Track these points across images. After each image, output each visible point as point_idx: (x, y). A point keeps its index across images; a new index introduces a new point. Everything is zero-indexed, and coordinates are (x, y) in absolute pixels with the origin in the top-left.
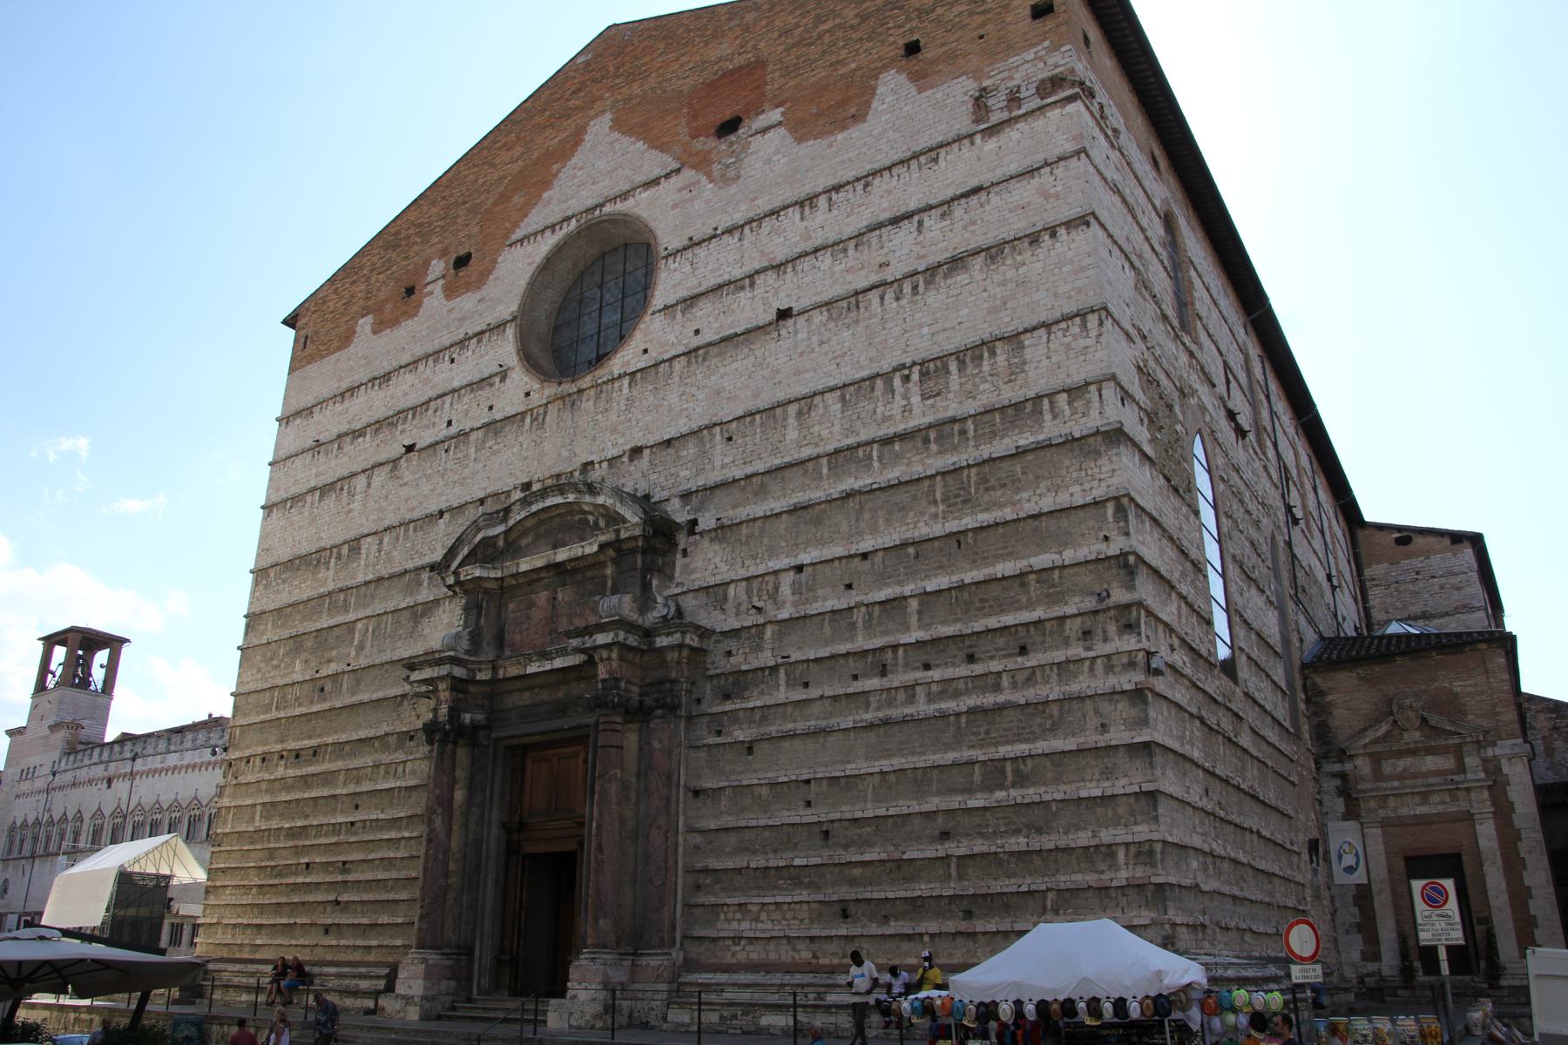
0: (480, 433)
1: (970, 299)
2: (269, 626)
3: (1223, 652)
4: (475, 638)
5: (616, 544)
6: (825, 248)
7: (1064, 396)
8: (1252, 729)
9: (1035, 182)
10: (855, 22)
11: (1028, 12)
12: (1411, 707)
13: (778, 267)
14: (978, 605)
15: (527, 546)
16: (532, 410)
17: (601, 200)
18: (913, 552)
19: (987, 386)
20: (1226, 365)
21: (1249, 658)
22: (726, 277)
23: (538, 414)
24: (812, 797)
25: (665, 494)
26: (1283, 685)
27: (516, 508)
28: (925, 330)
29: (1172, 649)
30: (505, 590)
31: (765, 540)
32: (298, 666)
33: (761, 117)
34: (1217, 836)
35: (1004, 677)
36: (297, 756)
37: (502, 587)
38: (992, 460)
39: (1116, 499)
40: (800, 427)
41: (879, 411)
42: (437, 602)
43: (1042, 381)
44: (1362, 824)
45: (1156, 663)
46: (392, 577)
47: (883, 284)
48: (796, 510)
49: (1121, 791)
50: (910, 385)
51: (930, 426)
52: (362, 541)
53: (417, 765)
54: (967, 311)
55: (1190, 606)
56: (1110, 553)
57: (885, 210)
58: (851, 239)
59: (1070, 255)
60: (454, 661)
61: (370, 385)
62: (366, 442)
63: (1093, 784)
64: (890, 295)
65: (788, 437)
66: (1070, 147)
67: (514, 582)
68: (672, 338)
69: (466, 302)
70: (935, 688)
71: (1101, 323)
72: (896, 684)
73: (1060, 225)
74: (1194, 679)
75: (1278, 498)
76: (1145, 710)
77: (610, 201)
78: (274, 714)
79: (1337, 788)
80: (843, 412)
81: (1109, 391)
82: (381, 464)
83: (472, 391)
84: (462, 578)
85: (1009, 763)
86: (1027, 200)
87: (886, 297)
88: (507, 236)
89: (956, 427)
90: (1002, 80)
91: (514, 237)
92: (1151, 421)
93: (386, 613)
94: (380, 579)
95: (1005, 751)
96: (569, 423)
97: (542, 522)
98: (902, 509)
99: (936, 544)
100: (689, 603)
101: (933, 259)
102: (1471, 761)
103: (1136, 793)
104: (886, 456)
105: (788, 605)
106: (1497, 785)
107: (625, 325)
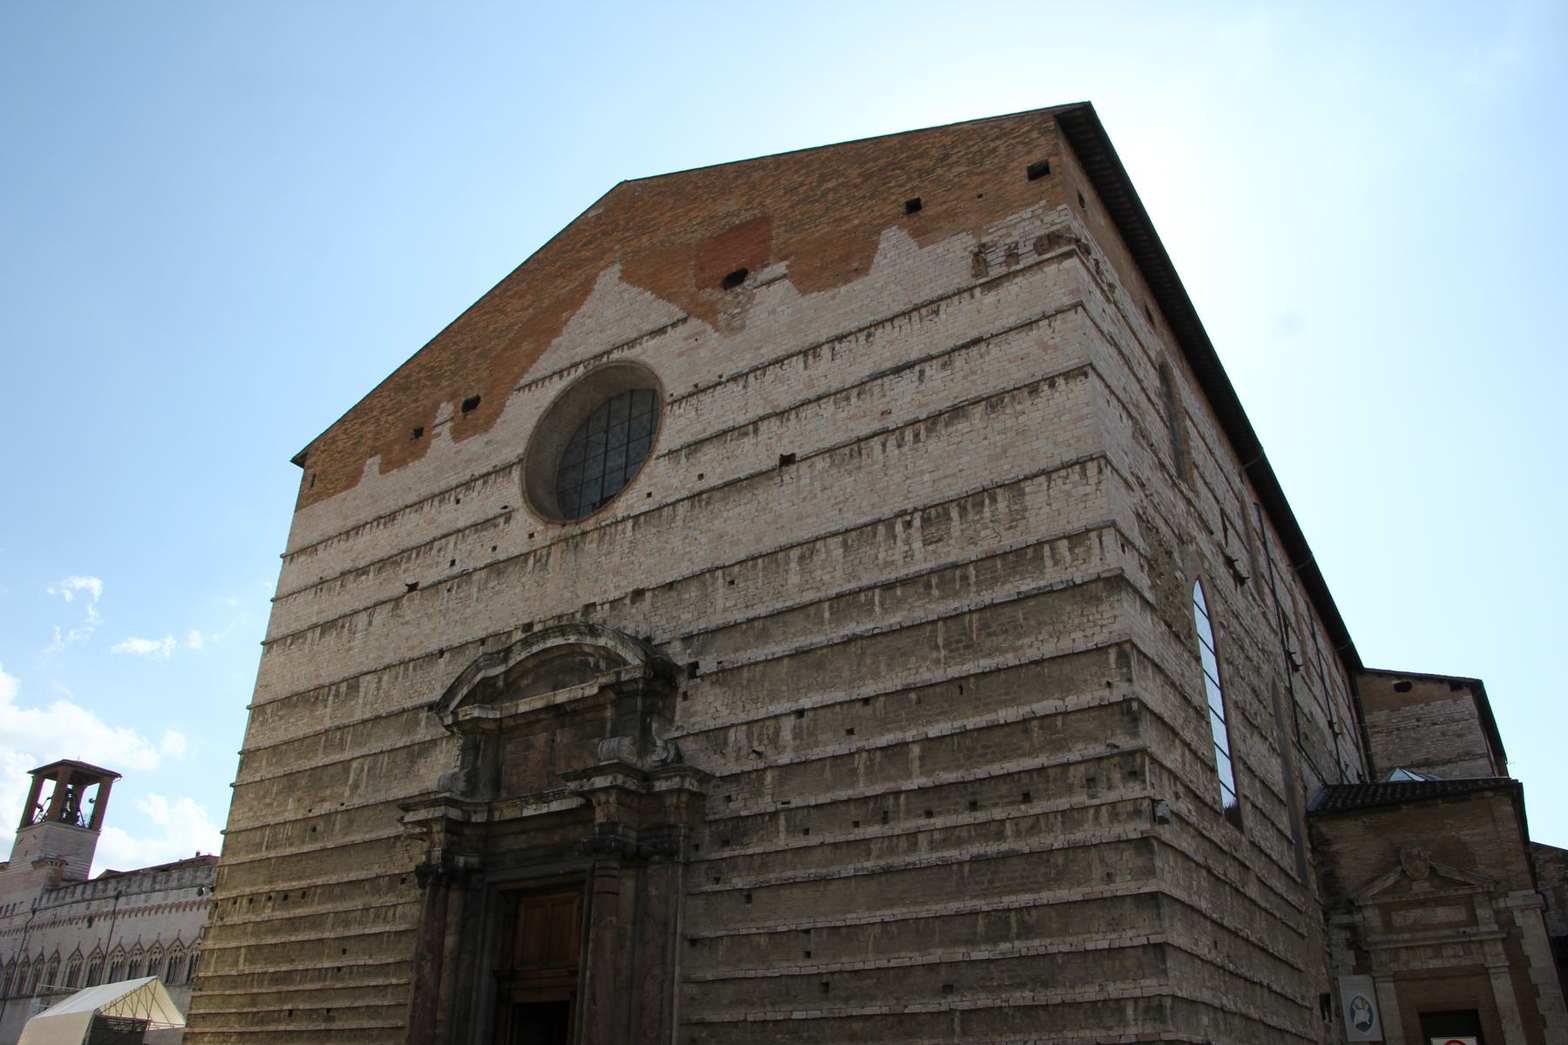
0: (483, 574)
1: (971, 447)
2: (264, 763)
3: (1228, 799)
4: (472, 779)
5: (617, 687)
6: (828, 395)
7: (1065, 543)
8: (1258, 879)
9: (1034, 333)
10: (858, 181)
11: (1025, 173)
12: (1419, 856)
13: (782, 415)
14: (980, 751)
15: (528, 686)
16: (535, 551)
17: (609, 347)
18: (915, 698)
19: (988, 532)
20: (1222, 510)
21: (1254, 806)
22: (730, 424)
23: (541, 556)
24: (811, 947)
25: (667, 637)
26: (1289, 834)
27: (517, 648)
28: (927, 477)
29: (1177, 797)
30: (503, 730)
31: (767, 684)
32: (291, 805)
33: (766, 270)
34: (1226, 991)
35: (1008, 825)
36: (286, 898)
37: (500, 729)
38: (993, 606)
39: (1119, 645)
40: (802, 572)
41: (881, 556)
42: (433, 742)
43: (1043, 528)
44: (1374, 978)
45: (1161, 811)
46: (390, 716)
47: (886, 432)
48: (798, 654)
49: (1128, 944)
50: (911, 531)
51: (932, 572)
52: (362, 679)
53: (407, 909)
54: (968, 458)
55: (1194, 753)
56: (1113, 699)
57: (887, 360)
58: (853, 387)
59: (1068, 404)
60: (449, 802)
61: (375, 524)
62: (369, 580)
63: (1100, 936)
64: (892, 442)
65: (790, 582)
66: (1068, 301)
67: (513, 723)
68: (675, 482)
69: (474, 444)
70: (937, 836)
71: (1100, 471)
72: (897, 831)
73: (1058, 376)
74: (1200, 827)
75: (1278, 644)
76: (1152, 859)
77: (618, 348)
78: (264, 854)
79: (1347, 940)
80: (845, 557)
81: (1109, 537)
82: (384, 602)
83: (476, 531)
84: (460, 718)
85: (1013, 913)
86: (1026, 351)
87: (888, 444)
88: (515, 381)
89: (958, 573)
90: (1001, 237)
91: (523, 382)
92: (1151, 568)
93: (382, 752)
94: (378, 718)
95: (1008, 901)
96: (572, 565)
97: (543, 663)
98: (904, 654)
99: (938, 689)
100: (689, 747)
101: (933, 408)
102: (1483, 913)
103: (1143, 946)
104: (888, 602)
105: (789, 749)
106: (1511, 938)
107: (631, 469)
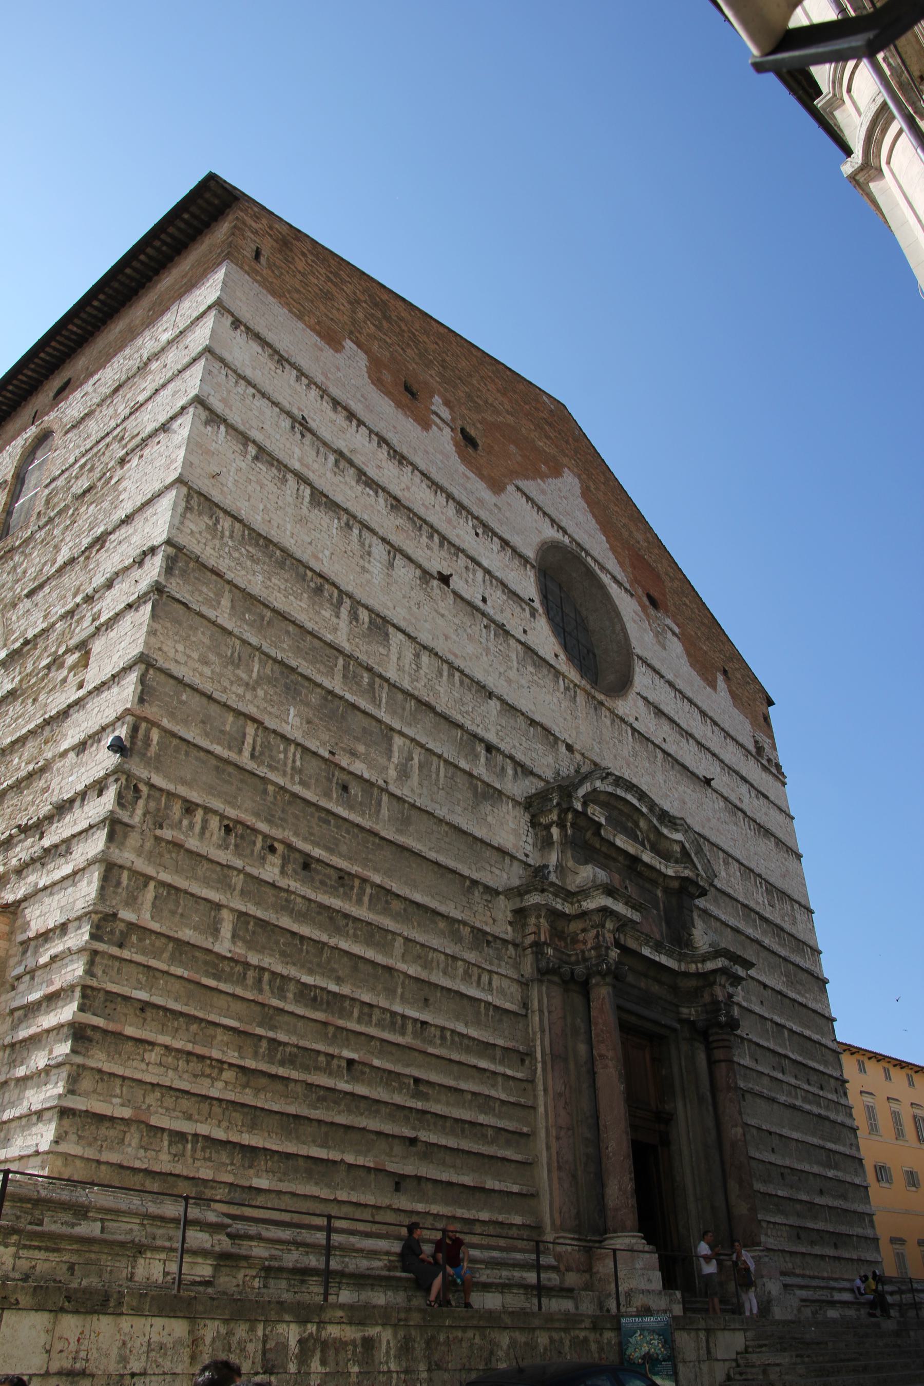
67: (598, 846)
